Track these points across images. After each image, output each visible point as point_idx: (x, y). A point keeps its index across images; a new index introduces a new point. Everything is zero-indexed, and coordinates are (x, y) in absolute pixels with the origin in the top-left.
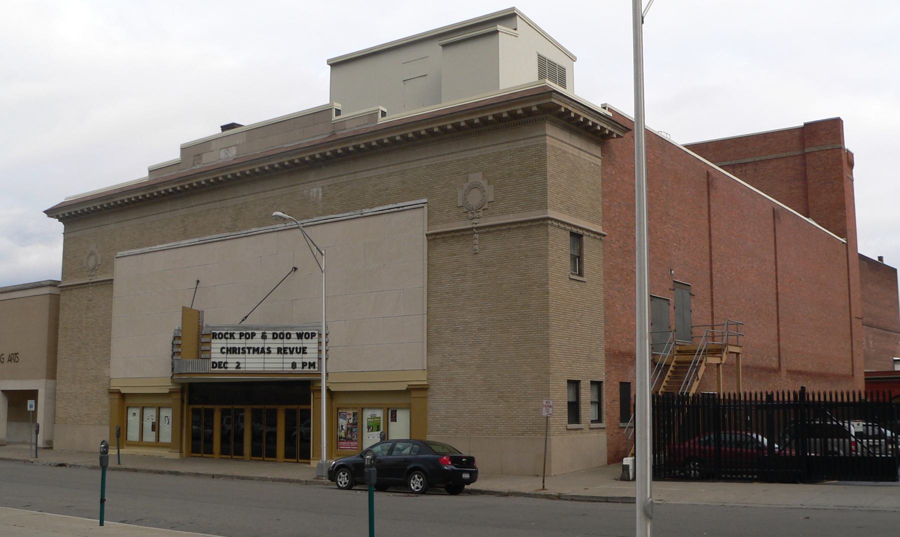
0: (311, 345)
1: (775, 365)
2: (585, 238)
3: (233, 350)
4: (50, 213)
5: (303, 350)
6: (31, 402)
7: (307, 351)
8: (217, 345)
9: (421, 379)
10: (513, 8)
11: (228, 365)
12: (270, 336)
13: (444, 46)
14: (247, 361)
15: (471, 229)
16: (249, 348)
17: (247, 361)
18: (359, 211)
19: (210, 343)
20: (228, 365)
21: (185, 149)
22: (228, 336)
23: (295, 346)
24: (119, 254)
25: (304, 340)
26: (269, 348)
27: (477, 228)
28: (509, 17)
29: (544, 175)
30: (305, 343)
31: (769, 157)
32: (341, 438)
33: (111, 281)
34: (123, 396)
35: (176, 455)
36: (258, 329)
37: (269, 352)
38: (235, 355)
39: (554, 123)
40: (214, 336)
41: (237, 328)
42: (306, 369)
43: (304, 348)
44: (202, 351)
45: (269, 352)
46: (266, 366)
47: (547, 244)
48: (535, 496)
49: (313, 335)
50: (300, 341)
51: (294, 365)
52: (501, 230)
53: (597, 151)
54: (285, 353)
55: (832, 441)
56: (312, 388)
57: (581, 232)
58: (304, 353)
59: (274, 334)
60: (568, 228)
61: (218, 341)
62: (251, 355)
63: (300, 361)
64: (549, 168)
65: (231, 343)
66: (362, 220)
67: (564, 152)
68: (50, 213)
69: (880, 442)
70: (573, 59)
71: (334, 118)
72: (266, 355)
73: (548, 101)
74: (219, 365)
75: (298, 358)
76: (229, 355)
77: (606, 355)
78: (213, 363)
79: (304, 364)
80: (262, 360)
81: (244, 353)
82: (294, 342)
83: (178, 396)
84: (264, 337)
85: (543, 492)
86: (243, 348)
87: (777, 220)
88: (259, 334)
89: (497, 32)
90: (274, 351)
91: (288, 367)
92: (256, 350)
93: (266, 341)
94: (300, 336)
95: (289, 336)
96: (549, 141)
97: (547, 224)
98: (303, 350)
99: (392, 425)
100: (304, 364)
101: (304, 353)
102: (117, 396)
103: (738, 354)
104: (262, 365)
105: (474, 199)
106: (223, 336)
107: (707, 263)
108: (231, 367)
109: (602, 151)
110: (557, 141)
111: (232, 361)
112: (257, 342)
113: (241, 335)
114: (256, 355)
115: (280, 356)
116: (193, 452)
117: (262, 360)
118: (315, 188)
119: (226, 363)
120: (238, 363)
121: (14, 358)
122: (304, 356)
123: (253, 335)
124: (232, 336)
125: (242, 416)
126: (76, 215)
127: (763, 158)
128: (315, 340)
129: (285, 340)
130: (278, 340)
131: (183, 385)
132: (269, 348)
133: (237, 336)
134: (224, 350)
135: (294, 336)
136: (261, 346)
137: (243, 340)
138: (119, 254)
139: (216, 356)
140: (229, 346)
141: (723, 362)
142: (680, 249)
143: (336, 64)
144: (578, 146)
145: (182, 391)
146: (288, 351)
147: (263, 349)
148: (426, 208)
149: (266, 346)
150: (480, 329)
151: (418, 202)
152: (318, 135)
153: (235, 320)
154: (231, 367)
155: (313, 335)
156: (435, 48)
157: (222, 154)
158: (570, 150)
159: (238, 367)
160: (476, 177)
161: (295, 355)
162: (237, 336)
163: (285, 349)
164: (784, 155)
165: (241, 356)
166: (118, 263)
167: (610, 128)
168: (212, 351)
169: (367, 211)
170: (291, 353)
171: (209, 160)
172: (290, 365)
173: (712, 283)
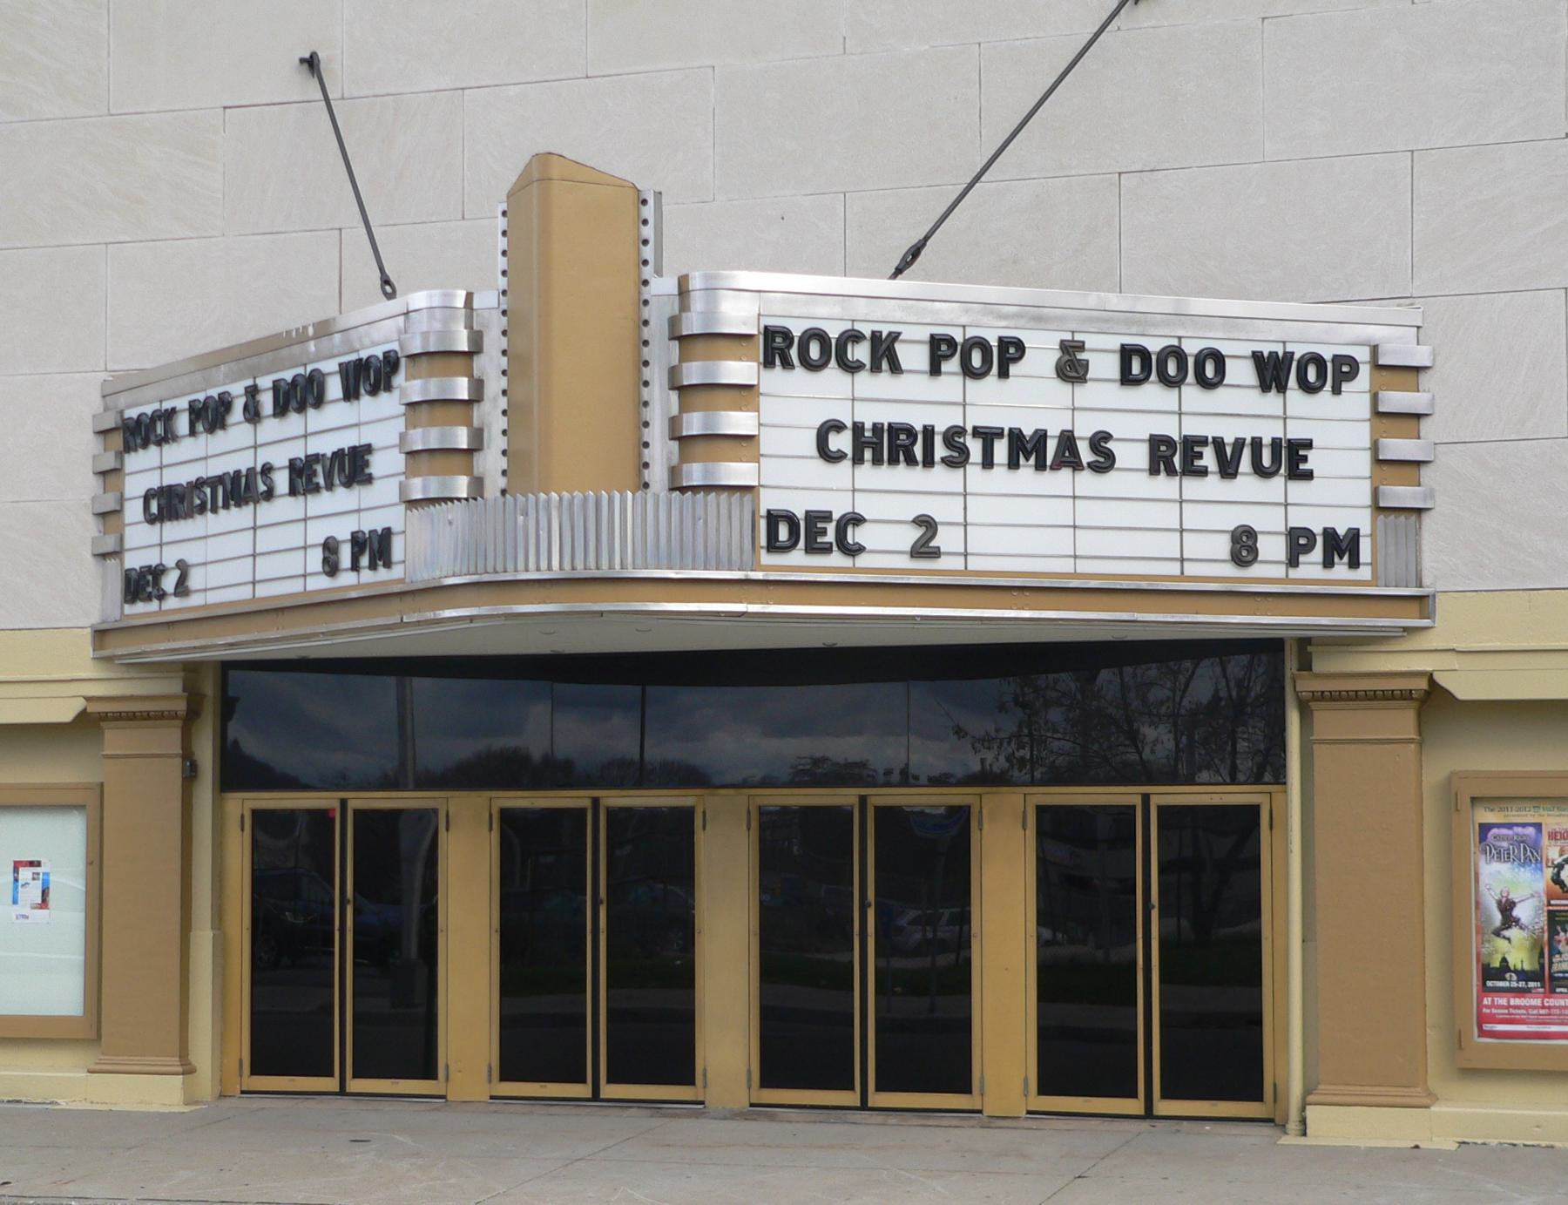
0: (1335, 425)
3: (893, 445)
7: (1314, 461)
11: (855, 535)
12: (1104, 365)
16: (988, 436)
20: (855, 535)
22: (861, 352)
23: (1247, 431)
26: (1099, 442)
30: (1303, 414)
32: (1492, 973)
36: (1039, 320)
37: (1105, 462)
38: (900, 476)
42: (1311, 566)
45: (1105, 462)
50: (1272, 402)
51: (1244, 545)
54: (1193, 470)
56: (1298, 684)
58: (1297, 473)
59: (1127, 353)
62: (1000, 475)
72: (1087, 482)
74: (809, 531)
75: (1259, 502)
76: (869, 475)
78: (773, 518)
79: (1299, 543)
80: (1061, 512)
81: (958, 459)
82: (1237, 411)
84: (1072, 367)
86: (953, 436)
88: (1042, 352)
90: (1132, 455)
91: (1210, 558)
92: (1027, 448)
93: (1086, 394)
94: (1271, 372)
95: (1209, 370)
98: (1291, 459)
100: (1299, 543)
111: (887, 500)
112: (1029, 399)
114: (1027, 470)
115: (1165, 485)
119: (856, 520)
120: (927, 524)
122: (1298, 489)
123: (1011, 351)
129: (1192, 394)
130: (1152, 394)
132: (1099, 442)
133: (913, 356)
134: (841, 442)
137: (951, 381)
139: (796, 481)
140: (869, 416)
146: (1209, 459)
147: (1068, 439)
149: (1084, 429)
154: (885, 546)
155: (1344, 369)
161: (1246, 484)
163: (1192, 445)
165: (941, 477)
170: (1228, 469)
172: (1223, 547)
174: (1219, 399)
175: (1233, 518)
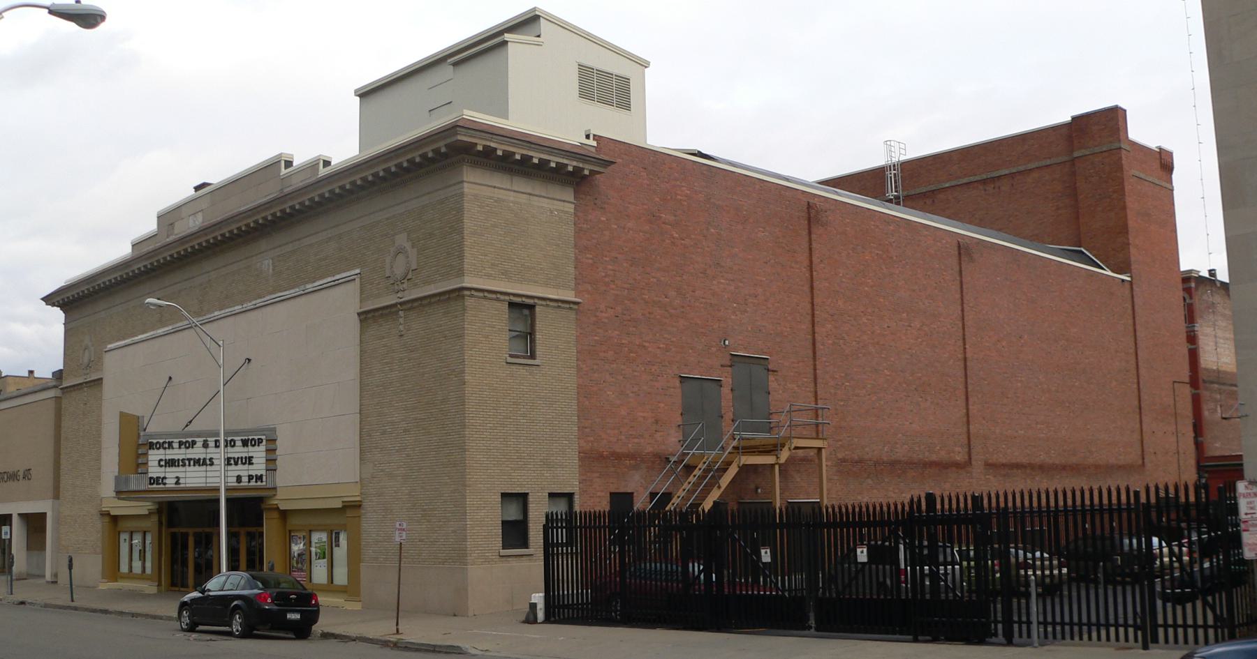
0: (259, 453)
2: (538, 309)
3: (171, 463)
4: (49, 300)
5: (249, 461)
6: (5, 529)
7: (254, 461)
8: (154, 456)
9: (353, 494)
10: (534, 9)
13: (455, 64)
14: (188, 475)
15: (395, 305)
16: (189, 460)
17: (188, 475)
18: (302, 287)
19: (146, 454)
21: (161, 217)
23: (240, 455)
24: (110, 346)
25: (250, 448)
26: (211, 459)
27: (401, 304)
28: (528, 22)
29: (461, 232)
31: (1030, 166)
33: (99, 381)
34: (115, 519)
35: (150, 588)
36: (199, 436)
38: (174, 469)
39: (475, 164)
40: (151, 446)
41: (176, 435)
42: (253, 483)
43: (251, 458)
44: (139, 465)
46: (209, 480)
47: (463, 320)
48: (385, 644)
49: (260, 441)
50: (245, 449)
51: (239, 479)
52: (423, 306)
53: (569, 194)
55: (884, 569)
56: (263, 506)
57: (530, 301)
58: (251, 463)
60: (502, 297)
61: (156, 451)
62: (192, 468)
63: (246, 473)
64: (468, 224)
65: (176, 453)
66: (303, 299)
67: (498, 201)
68: (49, 300)
69: (946, 569)
70: (644, 64)
71: (283, 171)
72: (209, 468)
73: (453, 139)
74: (156, 481)
75: (243, 470)
76: (168, 469)
77: (581, 459)
79: (250, 477)
80: (204, 474)
81: (184, 465)
83: (155, 519)
84: (205, 445)
85: (394, 638)
88: (200, 441)
89: (505, 43)
92: (197, 462)
93: (209, 450)
94: (245, 443)
96: (467, 188)
97: (463, 296)
98: (249, 461)
99: (336, 549)
100: (250, 477)
101: (251, 463)
102: (107, 519)
103: (820, 449)
104: (203, 480)
105: (399, 268)
106: (160, 446)
107: (806, 326)
108: (170, 483)
109: (575, 192)
110: (477, 186)
111: (171, 474)
112: (197, 452)
113: (181, 443)
114: (197, 468)
116: (173, 584)
117: (204, 474)
118: (264, 259)
121: (27, 474)
123: (194, 443)
124: (170, 444)
125: (208, 541)
126: (74, 300)
127: (1021, 168)
128: (262, 447)
131: (160, 504)
132: (211, 459)
133: (176, 445)
135: (239, 443)
136: (202, 457)
137: (183, 450)
138: (110, 346)
139: (154, 471)
140: (168, 457)
141: (782, 460)
142: (746, 311)
143: (366, 94)
144: (529, 191)
145: (159, 512)
148: (358, 281)
150: (405, 431)
151: (348, 274)
152: (266, 193)
153: (179, 427)
154: (170, 483)
155: (260, 441)
156: (447, 71)
157: (191, 223)
158: (511, 197)
159: (177, 483)
160: (402, 240)
161: (240, 467)
162: (176, 445)
164: (1048, 162)
165: (181, 469)
166: (108, 359)
167: (575, 163)
168: (264, 460)
169: (310, 287)
170: (236, 464)
171: (182, 229)
173: (814, 353)
174: (235, 449)
175: (237, 474)
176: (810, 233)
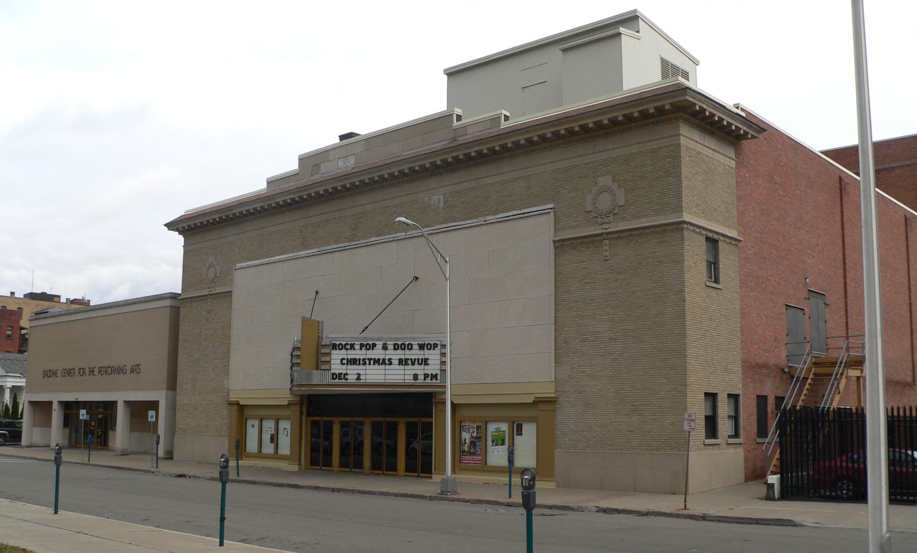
0: (434, 356)
1: (909, 379)
2: (720, 243)
3: (353, 362)
4: (171, 226)
5: (425, 362)
6: (152, 413)
7: (429, 362)
8: (337, 356)
9: (548, 391)
10: (635, 11)
11: (348, 377)
12: (391, 347)
15: (601, 235)
16: (370, 360)
18: (482, 219)
19: (329, 354)
20: (348, 377)
21: (304, 160)
22: (349, 347)
23: (417, 357)
24: (238, 265)
25: (426, 351)
26: (390, 360)
27: (607, 234)
28: (631, 19)
29: (678, 176)
30: (427, 354)
31: (893, 165)
32: (464, 452)
33: (229, 293)
34: (241, 408)
35: (295, 468)
36: (379, 340)
37: (390, 364)
38: (355, 367)
39: (686, 121)
40: (334, 347)
41: (357, 339)
42: (428, 380)
44: (320, 361)
45: (390, 364)
46: (387, 377)
47: (683, 249)
48: (677, 516)
49: (435, 346)
50: (422, 352)
51: (416, 377)
54: (406, 364)
56: (434, 400)
57: (716, 237)
58: (426, 364)
59: (395, 345)
61: (338, 352)
62: (372, 366)
64: (684, 170)
65: (352, 354)
67: (698, 153)
68: (171, 226)
70: (696, 63)
71: (455, 123)
72: (388, 367)
73: (680, 99)
75: (419, 370)
76: (349, 367)
78: (333, 374)
79: (426, 376)
81: (365, 364)
82: (415, 354)
83: (297, 408)
84: (385, 347)
85: (685, 512)
86: (364, 360)
87: (909, 228)
88: (379, 345)
90: (395, 362)
91: (409, 379)
92: (377, 361)
93: (388, 352)
94: (421, 347)
95: (410, 347)
96: (683, 141)
98: (425, 362)
99: (518, 439)
100: (426, 376)
101: (426, 364)
102: (235, 408)
105: (605, 202)
106: (342, 347)
107: (841, 271)
110: (690, 140)
111: (352, 372)
112: (378, 353)
113: (362, 346)
114: (377, 366)
115: (402, 367)
116: (312, 464)
118: (435, 194)
119: (346, 374)
120: (359, 375)
121: (135, 369)
122: (426, 367)
123: (374, 345)
126: (195, 227)
127: (886, 166)
128: (438, 351)
129: (407, 351)
130: (399, 351)
131: (302, 396)
132: (390, 360)
133: (357, 347)
134: (345, 361)
135: (416, 347)
136: (381, 357)
137: (364, 351)
138: (238, 265)
139: (337, 368)
140: (349, 357)
143: (453, 74)
145: (301, 403)
146: (409, 362)
147: (384, 360)
148: (552, 214)
149: (387, 358)
150: (611, 339)
152: (439, 141)
154: (352, 378)
155: (435, 346)
156: (555, 53)
157: (341, 164)
158: (705, 151)
159: (358, 379)
160: (605, 181)
161: (417, 366)
162: (357, 347)
163: (406, 360)
164: (909, 162)
165: (361, 367)
166: (238, 277)
167: (744, 128)
169: (490, 218)
170: (413, 364)
171: (328, 170)
172: (412, 377)
174: (412, 352)
175: (414, 372)
176: (841, 200)
